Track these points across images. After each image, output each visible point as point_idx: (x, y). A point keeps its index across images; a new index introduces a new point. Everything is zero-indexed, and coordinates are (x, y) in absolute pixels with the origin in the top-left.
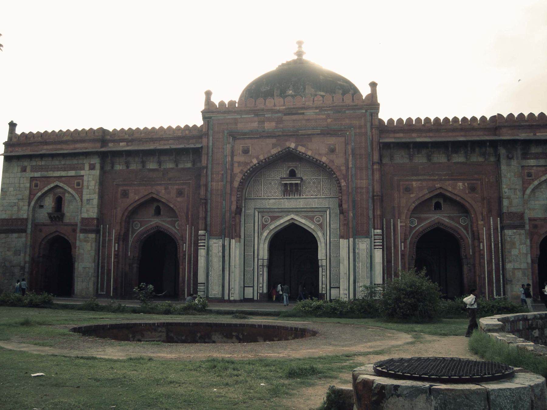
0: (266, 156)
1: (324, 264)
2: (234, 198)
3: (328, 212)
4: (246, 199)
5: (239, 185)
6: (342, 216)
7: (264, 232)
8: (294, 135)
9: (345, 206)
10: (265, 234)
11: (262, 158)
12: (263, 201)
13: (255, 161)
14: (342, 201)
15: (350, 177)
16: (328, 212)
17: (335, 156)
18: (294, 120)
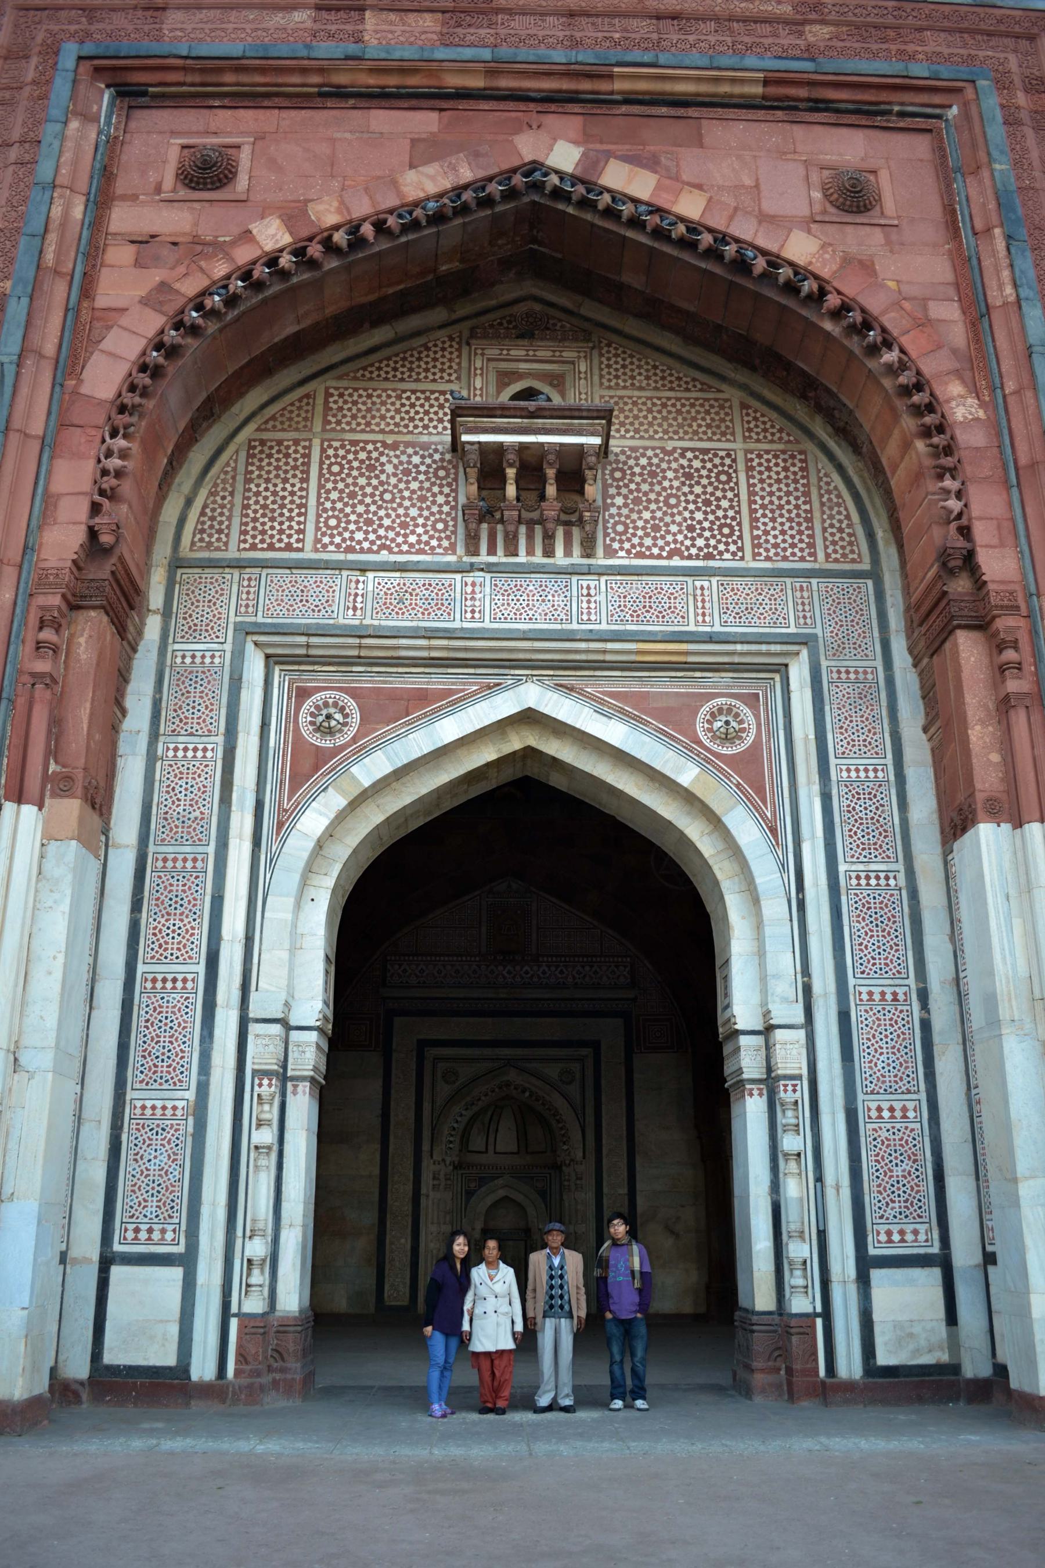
0: (362, 207)
1: (790, 1057)
2: (74, 477)
3: (799, 673)
4: (177, 564)
5: (132, 388)
6: (968, 649)
7: (299, 809)
8: (571, 98)
9: (997, 565)
10: (313, 821)
11: (331, 219)
12: (309, 579)
13: (272, 235)
14: (965, 532)
15: (1007, 365)
16: (799, 673)
17: (878, 235)
18: (572, 14)
